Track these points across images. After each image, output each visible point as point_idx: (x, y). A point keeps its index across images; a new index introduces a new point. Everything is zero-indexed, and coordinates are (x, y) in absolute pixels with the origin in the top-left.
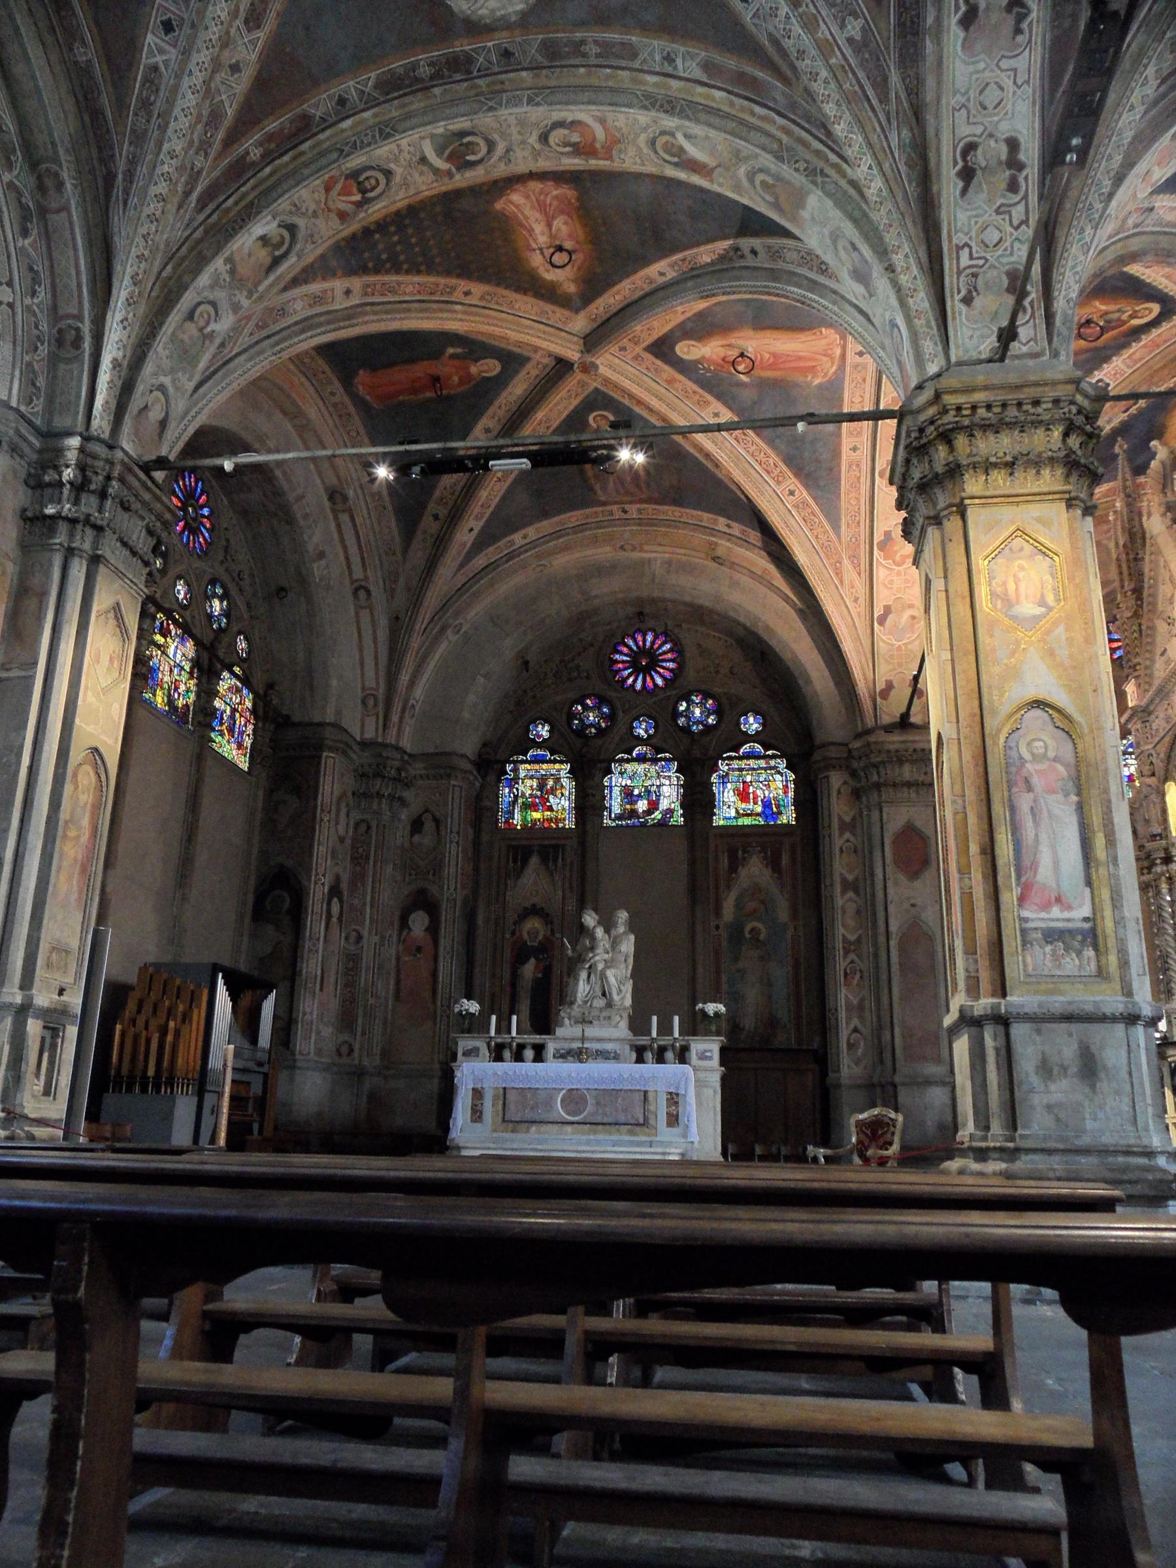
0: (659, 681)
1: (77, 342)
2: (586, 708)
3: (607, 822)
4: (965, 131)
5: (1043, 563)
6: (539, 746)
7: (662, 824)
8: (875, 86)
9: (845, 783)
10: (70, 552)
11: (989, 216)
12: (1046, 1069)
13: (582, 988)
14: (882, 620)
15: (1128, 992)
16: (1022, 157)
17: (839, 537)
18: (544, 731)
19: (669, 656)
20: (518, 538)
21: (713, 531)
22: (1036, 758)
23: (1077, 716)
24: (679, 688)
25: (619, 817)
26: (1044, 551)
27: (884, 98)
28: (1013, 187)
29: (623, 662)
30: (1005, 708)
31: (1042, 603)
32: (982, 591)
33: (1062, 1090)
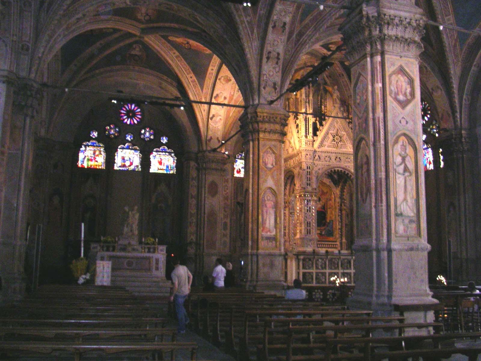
0: (136, 122)
1: (27, 50)
2: (111, 128)
3: (116, 168)
4: (269, 49)
5: (273, 155)
6: (94, 139)
7: (134, 171)
8: (251, 32)
9: (195, 165)
10: (26, 115)
11: (271, 69)
12: (264, 265)
13: (126, 229)
14: (211, 119)
15: (280, 250)
16: (280, 57)
17: (202, 91)
18: (95, 134)
19: (139, 113)
20: (97, 71)
21: (161, 79)
22: (268, 200)
23: (277, 192)
24: (142, 124)
25: (120, 167)
26: (274, 153)
27: (252, 35)
28: (277, 63)
29: (124, 113)
30: (263, 189)
31: (272, 165)
32: (261, 161)
33: (266, 270)
